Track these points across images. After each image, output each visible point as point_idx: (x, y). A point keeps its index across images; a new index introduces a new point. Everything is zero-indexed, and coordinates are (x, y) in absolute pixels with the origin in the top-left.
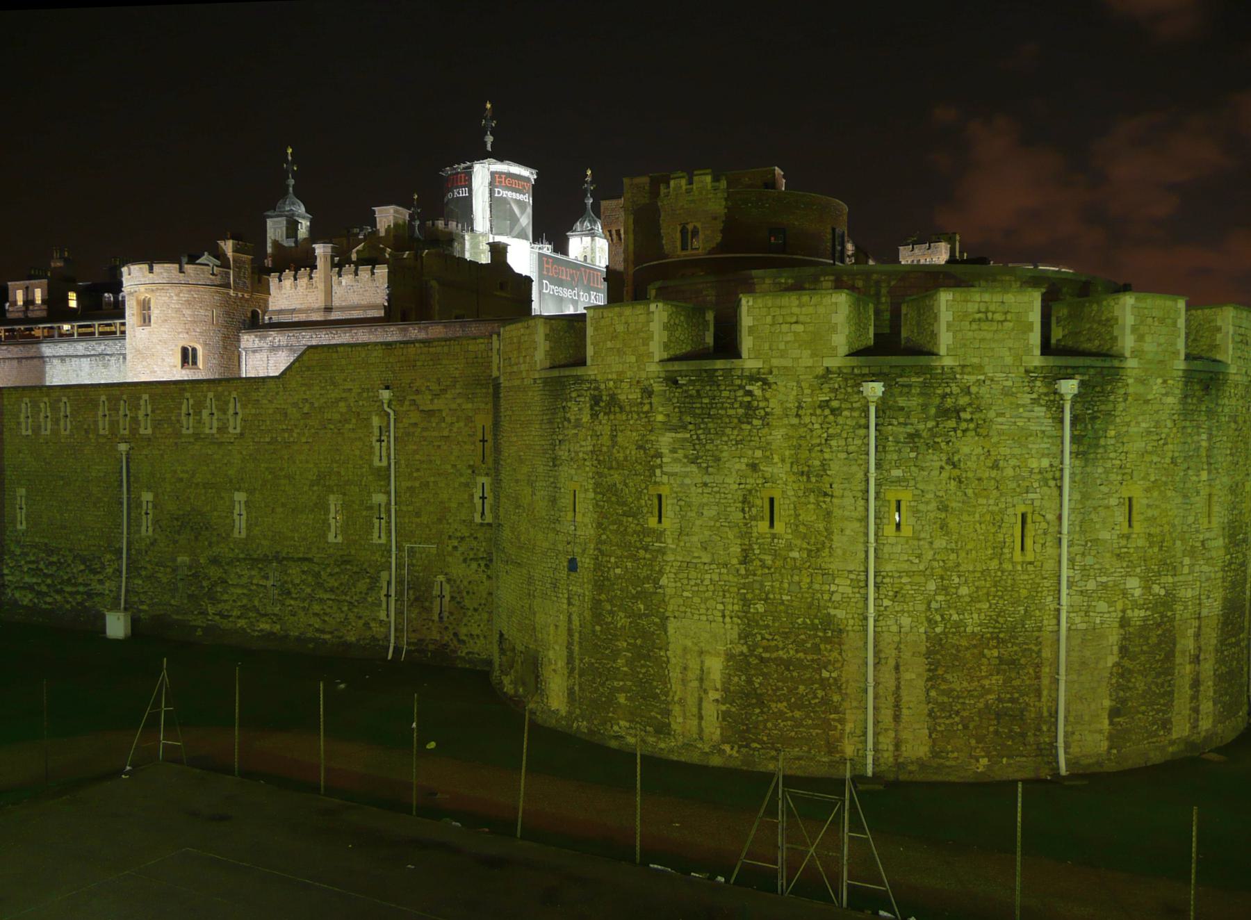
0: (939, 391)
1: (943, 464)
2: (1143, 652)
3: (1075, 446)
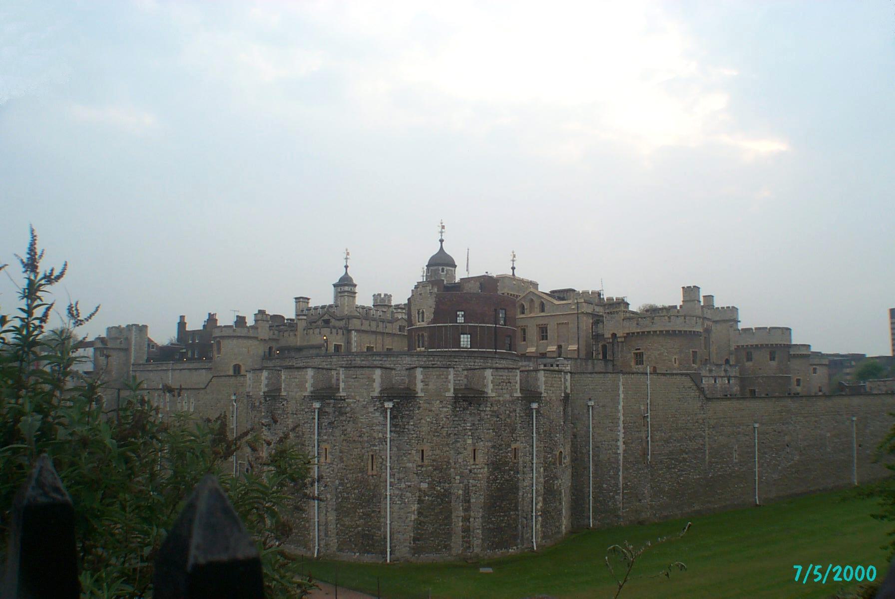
0: (340, 406)
2: (430, 515)
3: (393, 429)
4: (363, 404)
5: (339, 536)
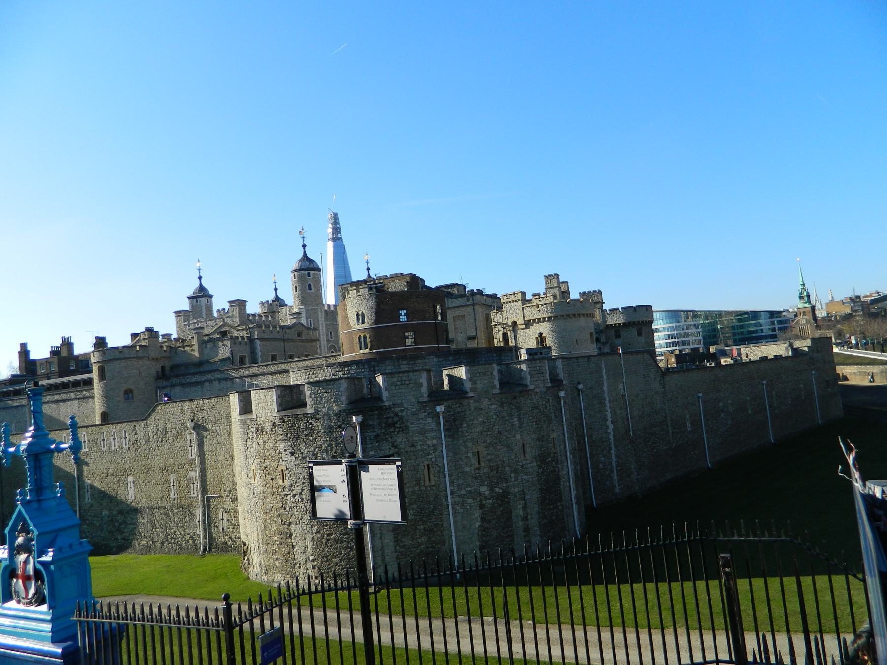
0: (385, 416)
1: (390, 447)
3: (447, 433)
4: (413, 411)
5: (399, 559)
